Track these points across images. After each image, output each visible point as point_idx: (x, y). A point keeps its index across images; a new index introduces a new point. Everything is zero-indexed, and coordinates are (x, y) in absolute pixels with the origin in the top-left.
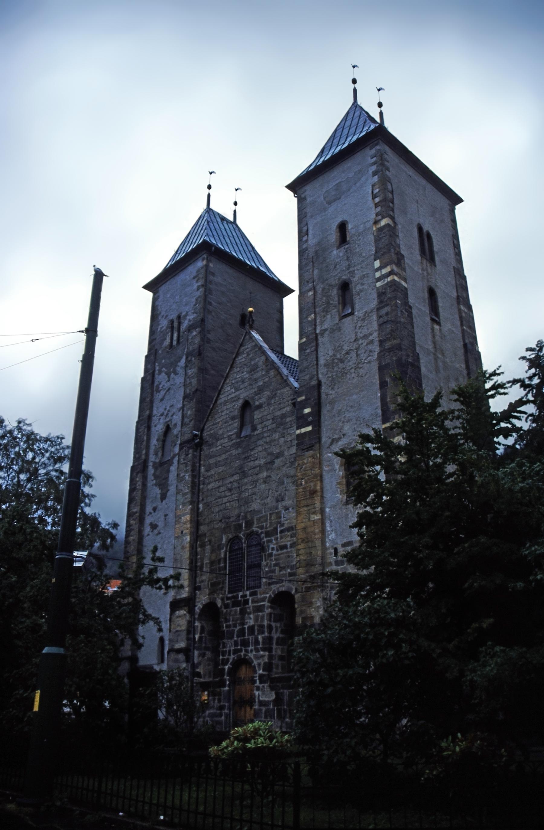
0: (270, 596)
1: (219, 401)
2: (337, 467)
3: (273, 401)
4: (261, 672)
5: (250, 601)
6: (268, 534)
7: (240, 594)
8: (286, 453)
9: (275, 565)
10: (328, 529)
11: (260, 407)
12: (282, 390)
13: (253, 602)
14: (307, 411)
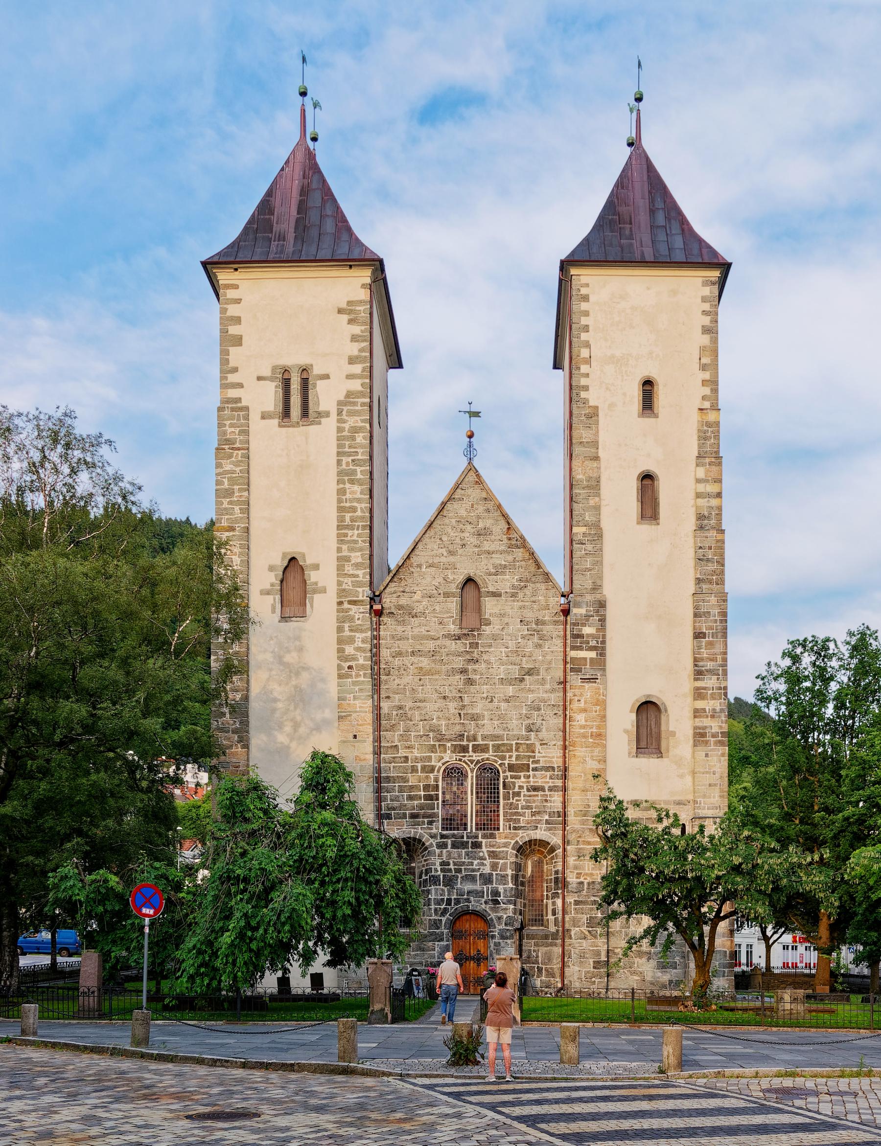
0: (517, 842)
4: (503, 926)
5: (483, 844)
6: (511, 768)
13: (486, 846)
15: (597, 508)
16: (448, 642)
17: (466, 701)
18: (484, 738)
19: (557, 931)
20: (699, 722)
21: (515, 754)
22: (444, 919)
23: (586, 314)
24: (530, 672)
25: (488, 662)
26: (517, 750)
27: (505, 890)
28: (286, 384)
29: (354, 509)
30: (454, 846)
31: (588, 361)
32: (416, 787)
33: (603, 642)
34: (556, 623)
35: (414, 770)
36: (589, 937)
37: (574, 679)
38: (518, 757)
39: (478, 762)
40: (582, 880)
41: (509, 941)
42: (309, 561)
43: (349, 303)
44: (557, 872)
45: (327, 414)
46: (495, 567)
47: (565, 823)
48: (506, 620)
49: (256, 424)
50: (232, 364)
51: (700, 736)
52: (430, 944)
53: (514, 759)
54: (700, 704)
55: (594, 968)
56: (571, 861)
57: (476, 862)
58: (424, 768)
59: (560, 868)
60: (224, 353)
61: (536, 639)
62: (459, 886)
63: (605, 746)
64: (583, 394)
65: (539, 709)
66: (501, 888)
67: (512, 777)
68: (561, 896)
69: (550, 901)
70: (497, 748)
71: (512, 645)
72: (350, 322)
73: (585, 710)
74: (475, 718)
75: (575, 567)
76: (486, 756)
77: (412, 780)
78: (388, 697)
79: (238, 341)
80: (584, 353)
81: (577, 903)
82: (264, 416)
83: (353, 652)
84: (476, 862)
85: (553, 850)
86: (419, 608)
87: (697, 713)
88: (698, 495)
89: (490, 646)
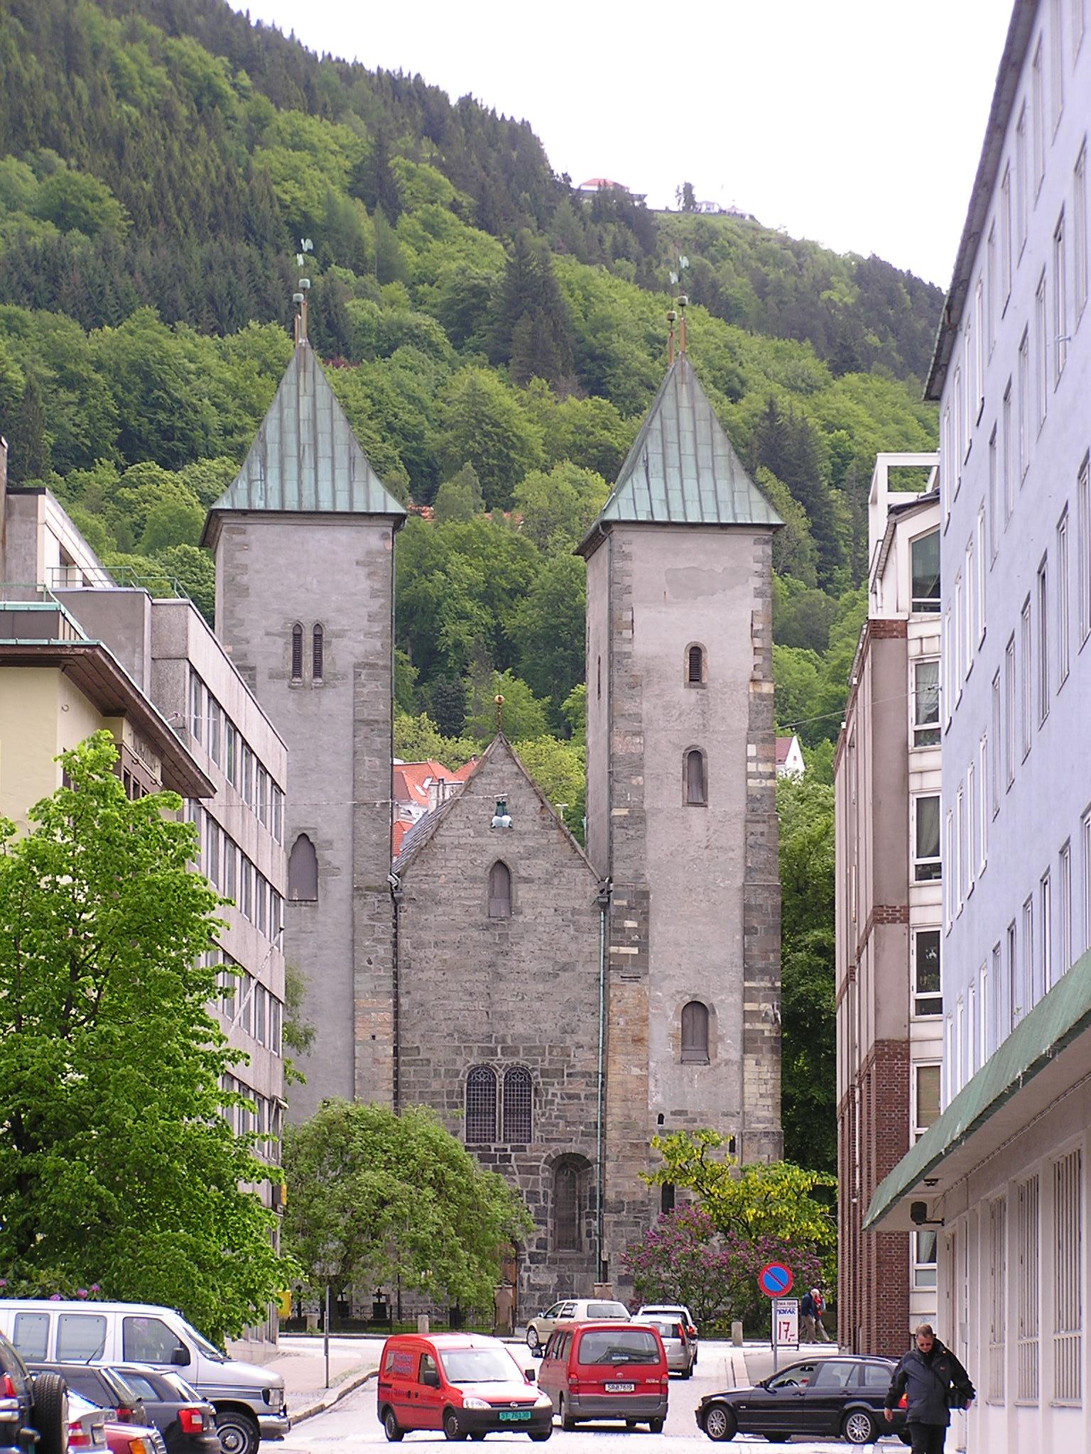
1: (438, 840)
2: (671, 1014)
3: (556, 881)
4: (534, 1249)
6: (544, 1073)
7: (493, 1146)
8: (580, 968)
9: (556, 1117)
10: (652, 1088)
11: (527, 880)
12: (575, 871)
13: (516, 1160)
14: (630, 924)
16: (475, 934)
17: (496, 997)
18: (514, 1039)
20: (747, 1026)
24: (565, 967)
25: (518, 954)
28: (297, 637)
33: (647, 936)
35: (437, 1074)
37: (615, 978)
38: (551, 1062)
41: (541, 1266)
43: (369, 553)
45: (344, 676)
51: (749, 1042)
53: (546, 1063)
54: (749, 1006)
58: (447, 1071)
61: (572, 931)
65: (575, 1009)
70: (528, 1050)
72: (370, 575)
74: (504, 1017)
75: (616, 853)
76: (515, 1060)
77: (435, 1085)
78: (408, 993)
80: (627, 616)
81: (617, 1224)
85: (589, 1164)
86: (445, 894)
87: (747, 1016)
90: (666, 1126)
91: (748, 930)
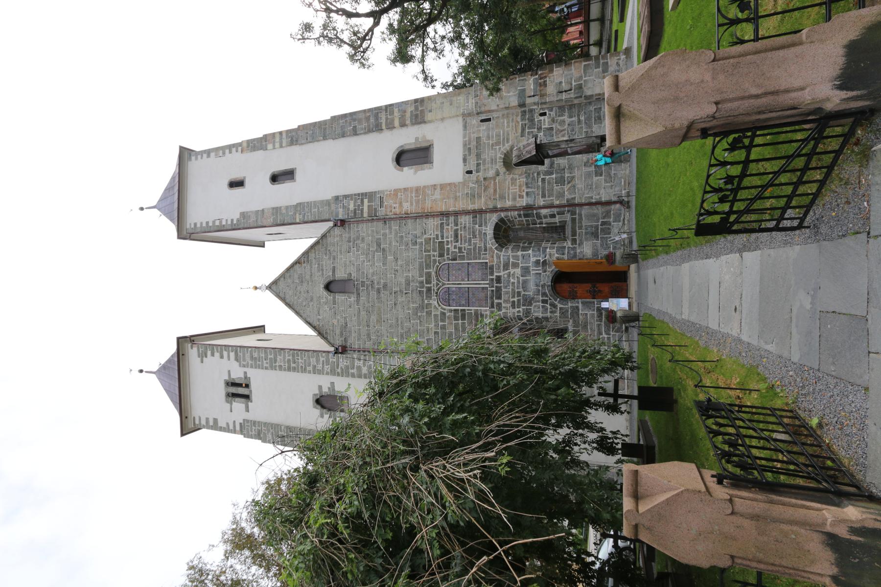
15: (287, 207)
16: (361, 302)
18: (421, 276)
19: (568, 211)
20: (408, 122)
21: (432, 253)
22: (559, 306)
23: (201, 223)
24: (379, 245)
25: (373, 274)
26: (429, 251)
27: (534, 256)
28: (235, 395)
29: (289, 360)
30: (499, 298)
31: (221, 220)
32: (456, 326)
33: (359, 194)
34: (349, 228)
35: (443, 327)
36: (573, 183)
37: (381, 212)
38: (434, 251)
39: (438, 280)
40: (524, 194)
41: (578, 251)
42: (317, 392)
44: (520, 216)
45: (245, 373)
46: (319, 271)
47: (481, 212)
48: (348, 263)
49: (250, 416)
50: (224, 425)
52: (581, 317)
54: (397, 123)
55: (601, 175)
56: (509, 203)
57: (512, 280)
58: (443, 320)
59: (516, 213)
60: (221, 429)
62: (531, 293)
63: (424, 187)
64: (235, 222)
65: (402, 237)
66: (533, 259)
67: (448, 254)
68: (539, 211)
69: (544, 220)
70: (428, 266)
71: (362, 258)
73: (401, 203)
74: (408, 283)
76: (433, 274)
79: (215, 420)
80: (217, 223)
81: (544, 196)
82: (247, 410)
83: (366, 368)
84: (512, 280)
85: (502, 220)
88: (281, 146)
89: (363, 273)
90: (473, 168)
91: (355, 133)
